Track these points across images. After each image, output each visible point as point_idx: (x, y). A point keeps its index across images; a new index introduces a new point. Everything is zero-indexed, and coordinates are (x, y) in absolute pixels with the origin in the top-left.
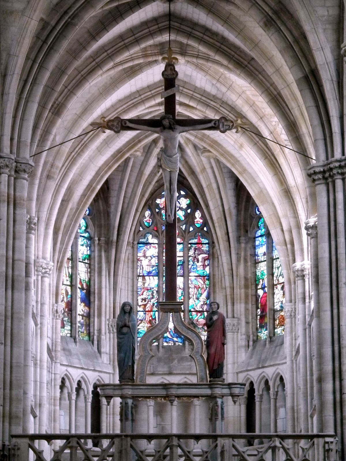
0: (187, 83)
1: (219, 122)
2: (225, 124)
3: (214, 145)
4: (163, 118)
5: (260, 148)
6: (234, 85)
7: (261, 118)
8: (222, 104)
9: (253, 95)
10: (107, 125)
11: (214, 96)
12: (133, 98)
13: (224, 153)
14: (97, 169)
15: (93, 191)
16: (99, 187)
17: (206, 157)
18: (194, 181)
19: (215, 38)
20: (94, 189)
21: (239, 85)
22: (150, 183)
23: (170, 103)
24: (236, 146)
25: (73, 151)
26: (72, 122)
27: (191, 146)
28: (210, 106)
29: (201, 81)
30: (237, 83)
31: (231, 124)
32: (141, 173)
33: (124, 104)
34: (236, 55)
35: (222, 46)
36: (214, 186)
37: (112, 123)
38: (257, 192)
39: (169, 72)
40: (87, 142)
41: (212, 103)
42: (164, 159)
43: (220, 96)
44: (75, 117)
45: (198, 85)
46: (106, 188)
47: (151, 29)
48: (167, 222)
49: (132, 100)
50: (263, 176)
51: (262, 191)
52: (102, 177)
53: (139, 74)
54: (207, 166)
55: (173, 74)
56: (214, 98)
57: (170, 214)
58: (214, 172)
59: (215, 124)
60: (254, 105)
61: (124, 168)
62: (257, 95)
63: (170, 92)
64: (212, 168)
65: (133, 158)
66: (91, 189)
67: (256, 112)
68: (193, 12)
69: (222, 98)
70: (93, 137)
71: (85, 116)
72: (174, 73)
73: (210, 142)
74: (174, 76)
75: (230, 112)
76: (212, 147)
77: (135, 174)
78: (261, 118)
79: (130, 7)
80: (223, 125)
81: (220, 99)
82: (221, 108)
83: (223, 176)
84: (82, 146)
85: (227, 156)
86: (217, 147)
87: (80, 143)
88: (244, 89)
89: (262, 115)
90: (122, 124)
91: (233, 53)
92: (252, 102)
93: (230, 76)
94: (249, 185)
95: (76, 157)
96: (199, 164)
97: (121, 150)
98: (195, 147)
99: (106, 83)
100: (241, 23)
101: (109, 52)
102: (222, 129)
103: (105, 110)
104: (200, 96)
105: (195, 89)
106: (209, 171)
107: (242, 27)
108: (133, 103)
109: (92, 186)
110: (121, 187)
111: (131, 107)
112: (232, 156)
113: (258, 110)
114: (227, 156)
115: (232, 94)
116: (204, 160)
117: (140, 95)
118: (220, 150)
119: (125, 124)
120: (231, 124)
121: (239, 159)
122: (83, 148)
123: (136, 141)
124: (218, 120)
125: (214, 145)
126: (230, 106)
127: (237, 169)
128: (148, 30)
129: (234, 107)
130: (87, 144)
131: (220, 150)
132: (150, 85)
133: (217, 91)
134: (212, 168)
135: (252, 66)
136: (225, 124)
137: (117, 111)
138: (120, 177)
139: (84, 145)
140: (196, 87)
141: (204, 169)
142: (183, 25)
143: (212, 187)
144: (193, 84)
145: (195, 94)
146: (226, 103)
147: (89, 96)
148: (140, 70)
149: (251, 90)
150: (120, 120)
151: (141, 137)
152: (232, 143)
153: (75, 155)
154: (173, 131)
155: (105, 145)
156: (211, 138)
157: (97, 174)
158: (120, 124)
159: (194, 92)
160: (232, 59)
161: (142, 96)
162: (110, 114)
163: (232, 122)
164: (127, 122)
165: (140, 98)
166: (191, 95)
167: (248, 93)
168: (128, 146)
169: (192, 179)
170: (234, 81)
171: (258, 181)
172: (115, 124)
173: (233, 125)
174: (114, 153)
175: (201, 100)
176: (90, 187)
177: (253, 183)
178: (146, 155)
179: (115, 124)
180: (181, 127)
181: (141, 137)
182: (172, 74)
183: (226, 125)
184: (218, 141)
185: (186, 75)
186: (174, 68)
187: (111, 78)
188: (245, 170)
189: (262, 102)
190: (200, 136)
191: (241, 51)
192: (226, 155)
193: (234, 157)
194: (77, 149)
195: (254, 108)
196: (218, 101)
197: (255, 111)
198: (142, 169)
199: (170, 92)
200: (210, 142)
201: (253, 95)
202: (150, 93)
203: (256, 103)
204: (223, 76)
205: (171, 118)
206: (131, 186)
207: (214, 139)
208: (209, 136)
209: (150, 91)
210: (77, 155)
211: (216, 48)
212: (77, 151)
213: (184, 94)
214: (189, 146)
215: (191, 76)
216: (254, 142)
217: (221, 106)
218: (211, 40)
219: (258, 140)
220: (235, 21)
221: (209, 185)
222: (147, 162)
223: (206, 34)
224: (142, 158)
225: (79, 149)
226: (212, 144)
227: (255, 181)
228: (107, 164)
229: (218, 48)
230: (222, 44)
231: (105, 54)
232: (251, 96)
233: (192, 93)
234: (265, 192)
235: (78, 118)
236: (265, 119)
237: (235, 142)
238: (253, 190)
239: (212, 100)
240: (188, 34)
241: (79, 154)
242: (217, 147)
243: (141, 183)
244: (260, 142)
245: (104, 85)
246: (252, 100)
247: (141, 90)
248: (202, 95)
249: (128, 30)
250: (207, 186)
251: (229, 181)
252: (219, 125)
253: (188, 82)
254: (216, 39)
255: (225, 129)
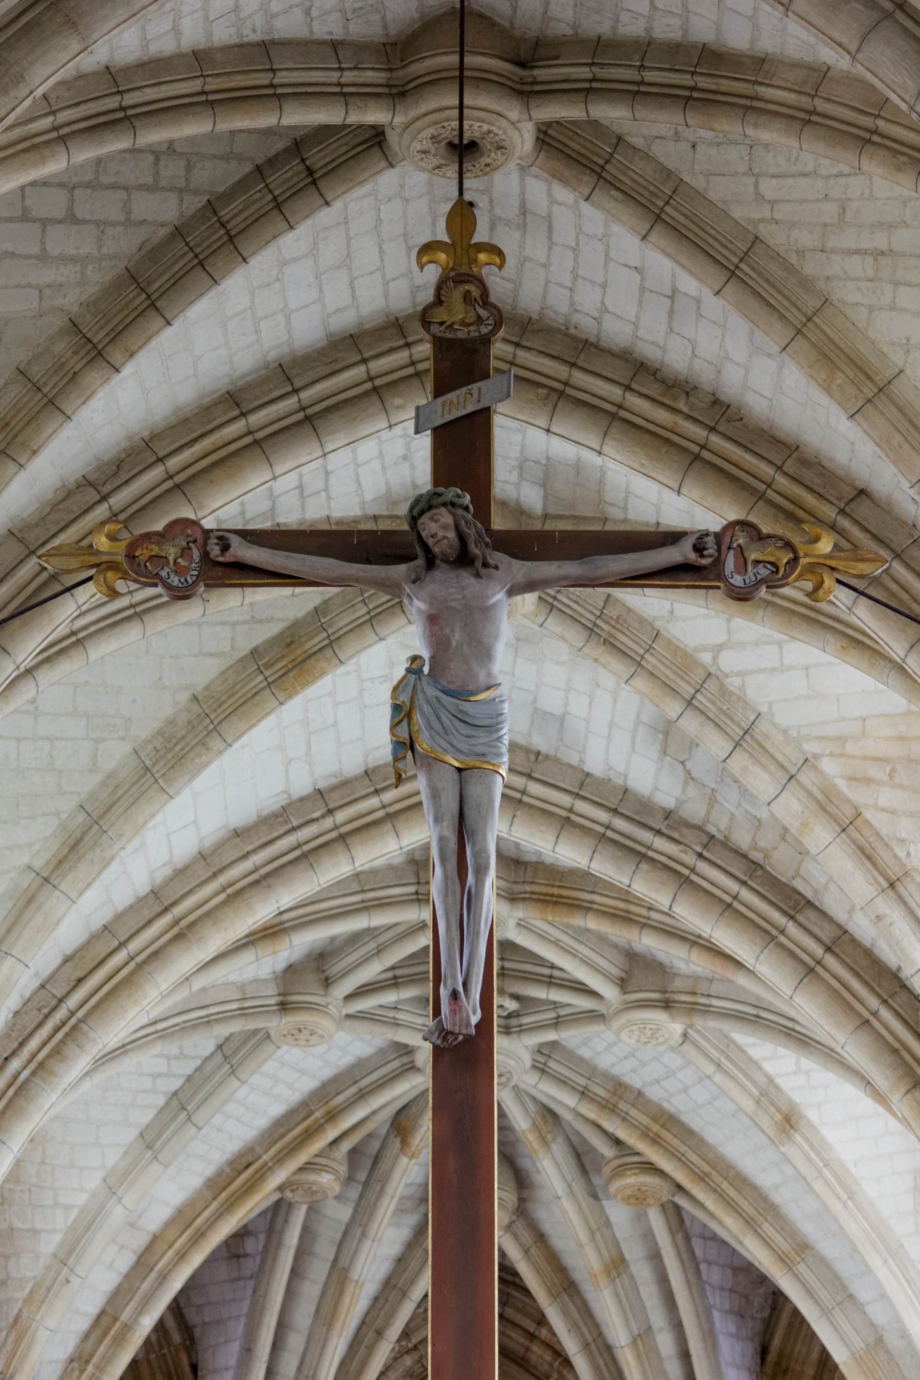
0: (547, 757)
1: (719, 544)
2: (753, 556)
3: (665, 1134)
4: (422, 507)
5: (886, 1043)
6: (763, 726)
7: (892, 885)
8: (705, 846)
9: (852, 779)
10: (131, 556)
11: (668, 814)
12: (295, 823)
13: (706, 1168)
14: (140, 1241)
15: (120, 1340)
16: (148, 1323)
17: (627, 1200)
18: (574, 1327)
19: (681, 405)
20: (128, 1328)
21: (785, 732)
22: (379, 1334)
23: (462, 450)
24: (765, 1122)
25: (14, 1053)
26: (10, 905)
27: (559, 1149)
28: (652, 860)
29: (609, 738)
30: (777, 720)
31: (785, 557)
32: (339, 1276)
33: (254, 851)
34: (782, 481)
35: (715, 439)
36: (665, 1343)
37: (155, 550)
38: (859, 1344)
39: (457, 312)
40: (80, 1014)
41: (660, 843)
42: (426, 708)
43: (694, 811)
44: (27, 880)
45: (595, 765)
46: (187, 1369)
47: (376, 366)
48: (445, 1034)
49: (294, 829)
50: (886, 1262)
51: (879, 1341)
52: (164, 1277)
53: (323, 673)
54: (634, 1252)
55: (479, 320)
56: (671, 823)
57: (460, 989)
58: (663, 1280)
59: (699, 549)
60: (859, 821)
61: (263, 1262)
62: (869, 781)
63: (461, 403)
64: (656, 1257)
65: (304, 1207)
66: (112, 1332)
67: (869, 858)
68: (575, 277)
69: (707, 821)
70: (110, 994)
71: (70, 877)
72: (483, 313)
73: (645, 1121)
74: (484, 330)
75: (744, 883)
76: (655, 1141)
77: (311, 1290)
78: (892, 885)
79: (275, 199)
80: (742, 564)
81: (699, 828)
82: (702, 867)
83: (704, 1296)
84: (57, 1030)
85: (725, 1185)
86: (675, 1142)
87: (47, 1017)
88: (810, 747)
89: (895, 871)
90: (205, 555)
91: (766, 470)
92: (849, 812)
93: (742, 688)
94: (825, 1311)
95: (27, 1081)
96: (598, 1236)
97: (251, 1159)
98: (583, 1160)
99: (171, 722)
100: (806, 284)
101: (174, 463)
102: (737, 580)
103: (168, 871)
104: (602, 816)
105: (583, 784)
106: (642, 1272)
107: (810, 303)
108: (299, 846)
109: (116, 1319)
110: (248, 1350)
111: (291, 862)
112: (742, 1182)
113: (878, 846)
114: (725, 1185)
115: (757, 769)
116: (619, 1214)
117: (330, 812)
118: (694, 1158)
119: (225, 547)
120: (785, 557)
121: (776, 1198)
122: (63, 1042)
123: (317, 1114)
124: (718, 536)
125: (665, 1134)
126: (745, 856)
127: (767, 1243)
128: (362, 368)
129: (756, 856)
130: (81, 1021)
131: (694, 1158)
132: (375, 769)
133: (686, 783)
134: (656, 1257)
135: (856, 522)
136: (753, 556)
137: (222, 880)
138: (245, 1307)
139: (66, 1029)
140: (588, 775)
141: (617, 1265)
142: (529, 349)
143: (655, 1349)
144: (574, 760)
145: (582, 807)
146: (726, 845)
147: (92, 782)
148: (328, 652)
149: (842, 755)
150: (199, 536)
151: (340, 1098)
152: (748, 1104)
153: (26, 1073)
154: (478, 575)
155: (174, 1118)
156: (648, 1102)
157: (143, 1262)
158: (196, 555)
159: (577, 796)
160: (761, 497)
161: (341, 816)
162: (190, 892)
163: (789, 545)
164: (235, 540)
165: (328, 823)
166: (564, 813)
167: (829, 767)
168: (282, 1136)
169: (566, 1314)
170: (764, 709)
171: (864, 1295)
172: (171, 552)
173: (796, 559)
174: (219, 1174)
175: (609, 834)
176: (106, 1323)
177: (839, 1304)
178: (361, 1196)
179: (171, 552)
180: (516, 564)
181: (340, 1098)
182: (471, 318)
183: (757, 562)
184: (684, 1118)
185: (539, 715)
186: (485, 292)
187: (195, 698)
188: (804, 1247)
189: (893, 812)
190: (601, 1092)
191: (805, 462)
192: (718, 1179)
193: (755, 1188)
194: (34, 1043)
195: (856, 835)
196: (689, 836)
197: (862, 850)
198: (344, 1261)
199: (461, 403)
200: (645, 1121)
201: (852, 779)
202: (374, 802)
203: (868, 815)
204: (711, 685)
205: (466, 508)
206: (295, 1342)
207: (666, 1105)
208: (640, 1093)
209: (377, 792)
210: (34, 1073)
211: (685, 450)
212: (33, 1056)
213: (531, 806)
214: (554, 1147)
215: (562, 720)
216: (859, 1015)
217: (700, 855)
218: (662, 416)
219: (873, 1002)
220: (773, 269)
221: (643, 1338)
222: (365, 1227)
223: (634, 386)
224: (344, 1213)
225: (44, 1044)
226: (656, 1128)
227: (851, 1296)
228: (186, 1221)
229: (696, 449)
230: (712, 429)
231: (157, 473)
232: (842, 784)
233: (565, 800)
234: (893, 1341)
235: (40, 887)
236: (907, 889)
237: (758, 1103)
238: (843, 1339)
239: (659, 832)
240: (552, 389)
241: (41, 1065)
242: (675, 1142)
243: (338, 1326)
244: (886, 1014)
245: (160, 733)
246: (849, 801)
247: (334, 788)
248: (615, 811)
249: (267, 366)
250: (634, 1342)
251: (733, 1329)
252: (718, 562)
253: (551, 753)
254: (686, 410)
255: (750, 577)
